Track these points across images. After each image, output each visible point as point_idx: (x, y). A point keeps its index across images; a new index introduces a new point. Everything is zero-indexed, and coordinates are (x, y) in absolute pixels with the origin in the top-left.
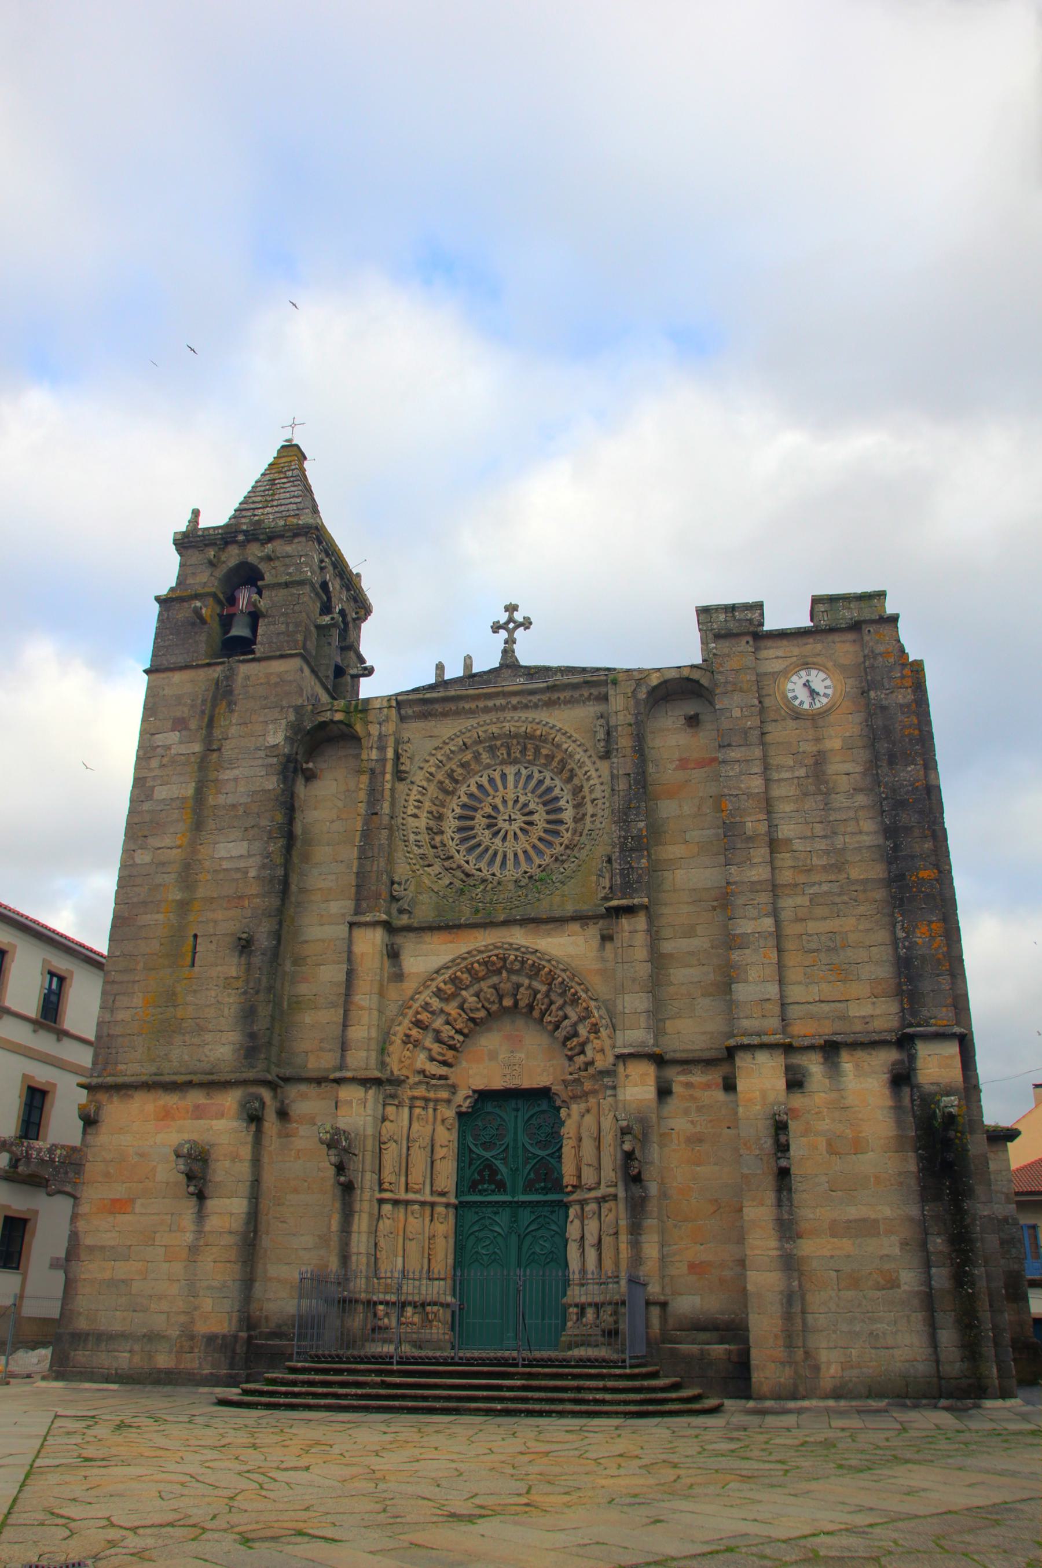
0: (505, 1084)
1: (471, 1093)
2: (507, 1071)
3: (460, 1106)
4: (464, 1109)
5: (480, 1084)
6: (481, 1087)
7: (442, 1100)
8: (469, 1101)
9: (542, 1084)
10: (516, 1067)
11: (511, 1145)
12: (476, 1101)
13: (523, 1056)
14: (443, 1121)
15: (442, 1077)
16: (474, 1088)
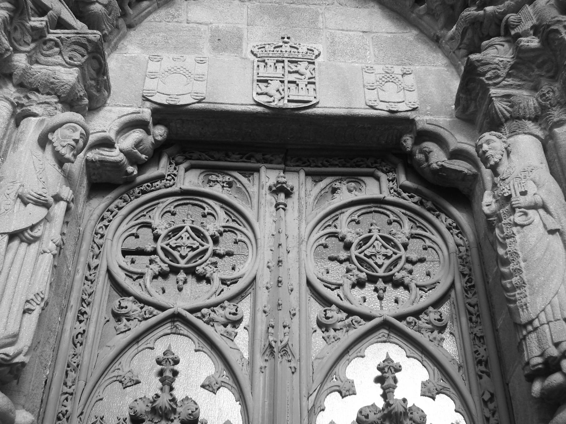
0: (263, 99)
1: (146, 114)
2: (264, 73)
3: (107, 143)
4: (115, 155)
5: (180, 91)
6: (182, 101)
7: (50, 88)
8: (136, 135)
9: (382, 110)
10: (301, 67)
11: (265, 278)
12: (158, 151)
13: (319, 47)
14: (44, 141)
15: (61, 24)
16: (162, 100)
